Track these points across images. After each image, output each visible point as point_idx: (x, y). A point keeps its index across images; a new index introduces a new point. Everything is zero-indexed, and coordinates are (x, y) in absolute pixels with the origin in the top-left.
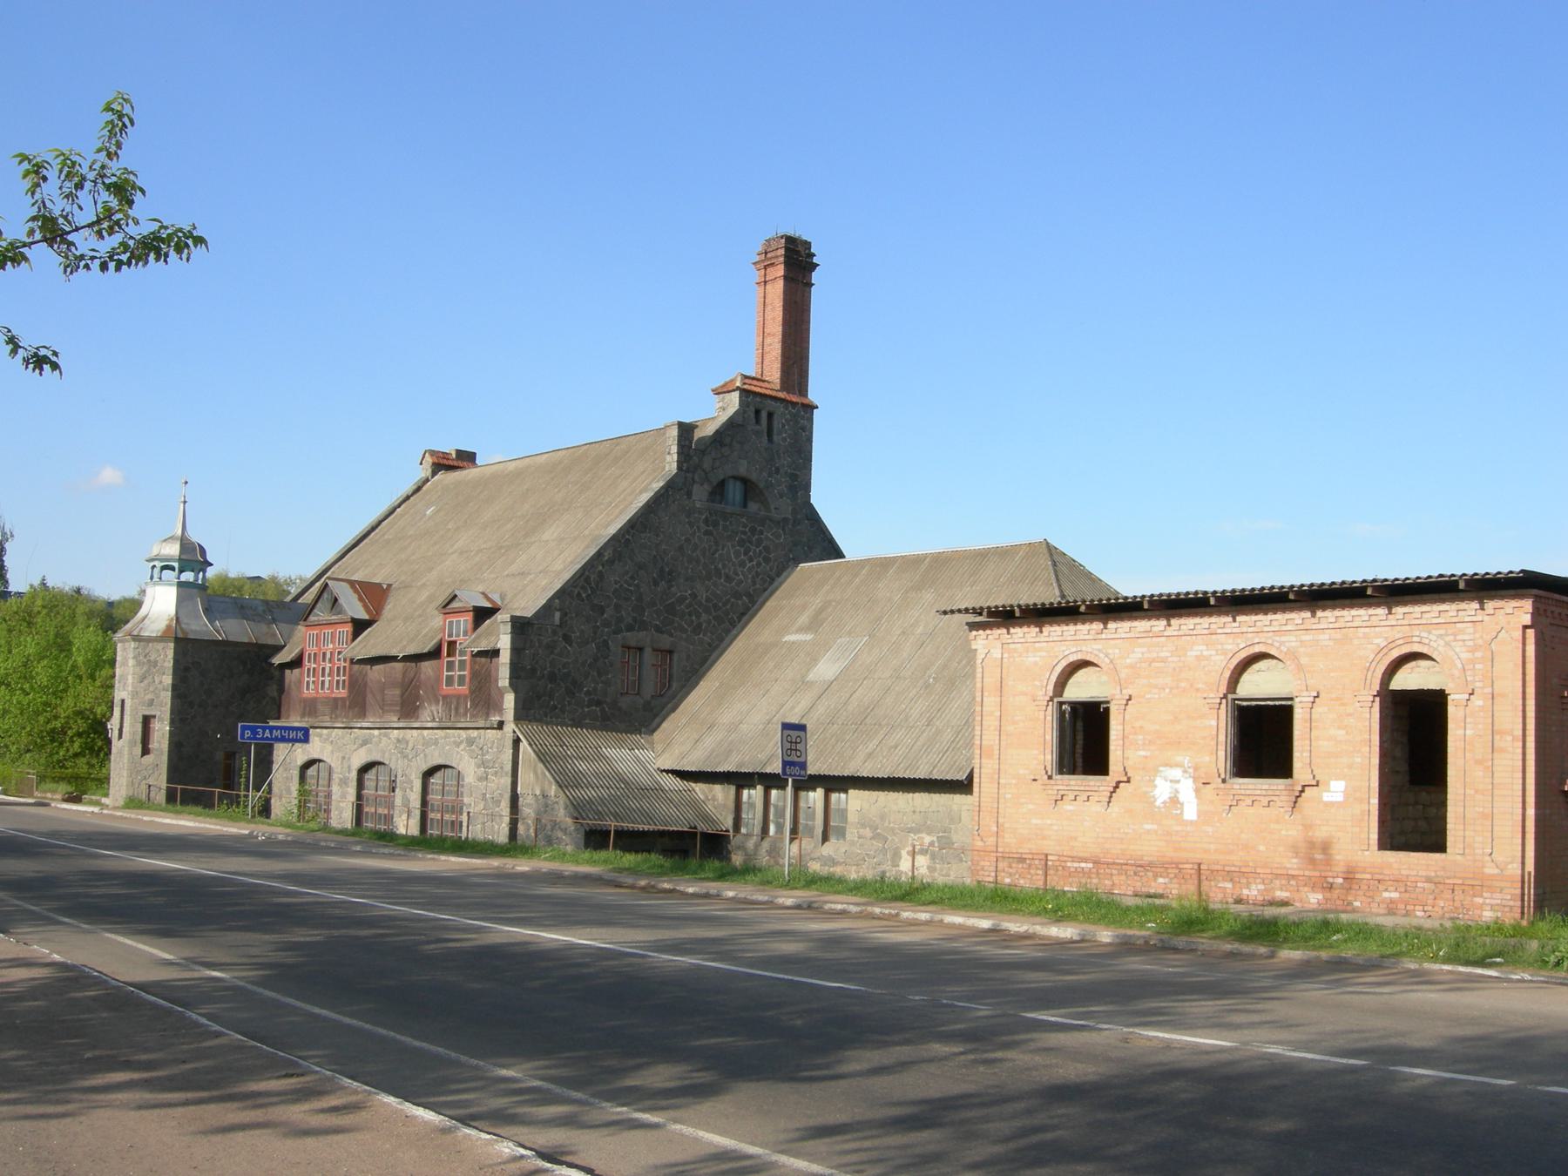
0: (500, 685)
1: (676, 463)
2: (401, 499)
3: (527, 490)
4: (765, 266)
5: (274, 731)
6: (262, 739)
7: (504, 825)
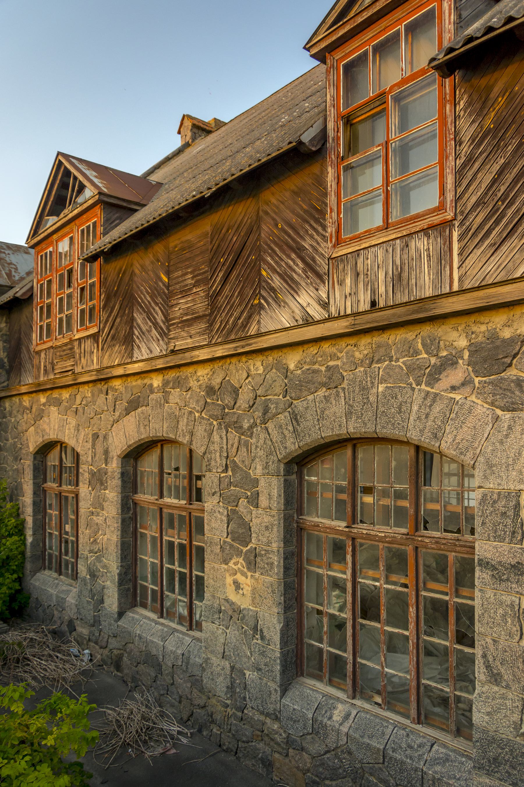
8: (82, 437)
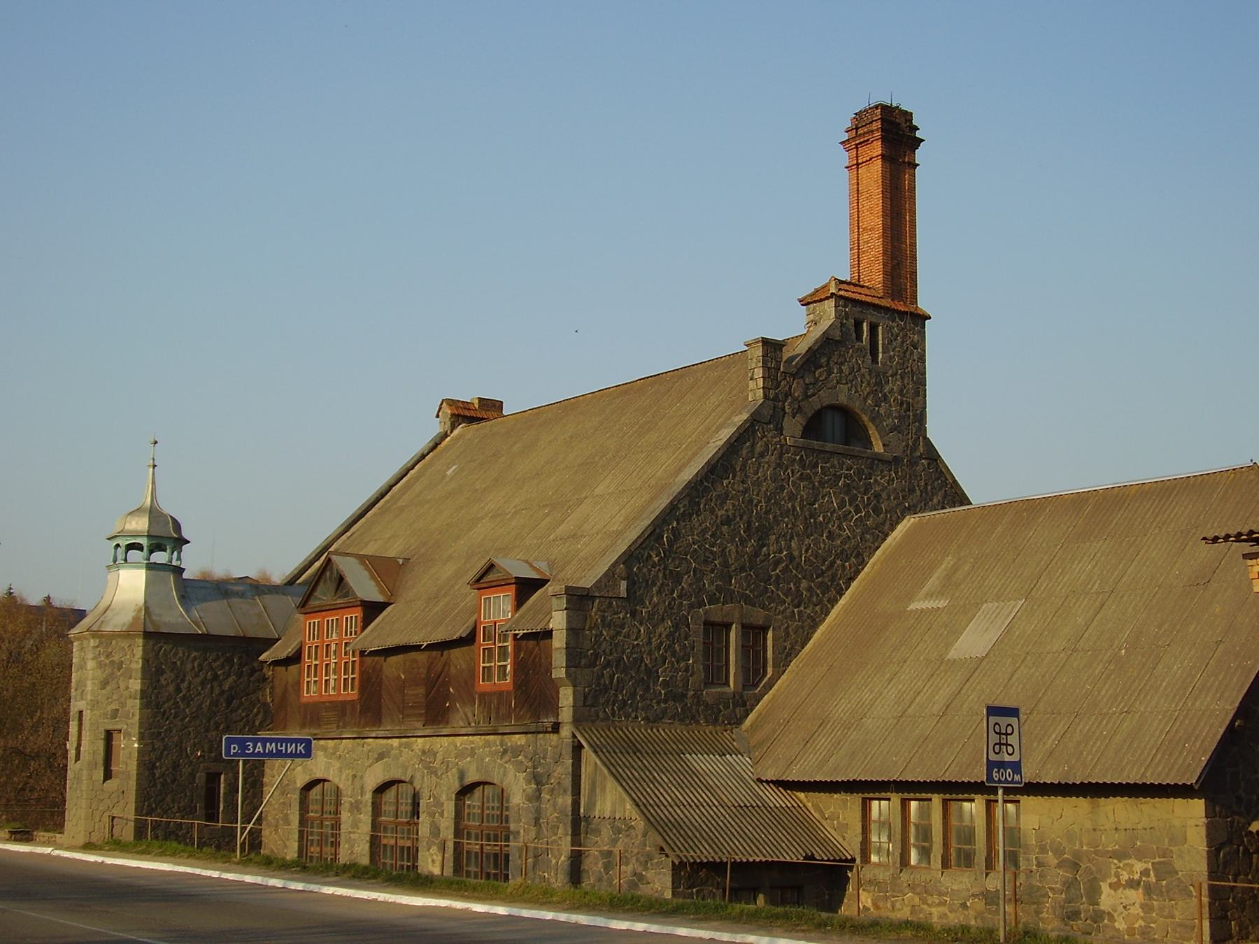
0: (553, 677)
1: (761, 390)
2: (415, 459)
3: (571, 437)
4: (857, 145)
5: (268, 744)
6: (253, 754)
7: (563, 858)
8: (344, 777)
